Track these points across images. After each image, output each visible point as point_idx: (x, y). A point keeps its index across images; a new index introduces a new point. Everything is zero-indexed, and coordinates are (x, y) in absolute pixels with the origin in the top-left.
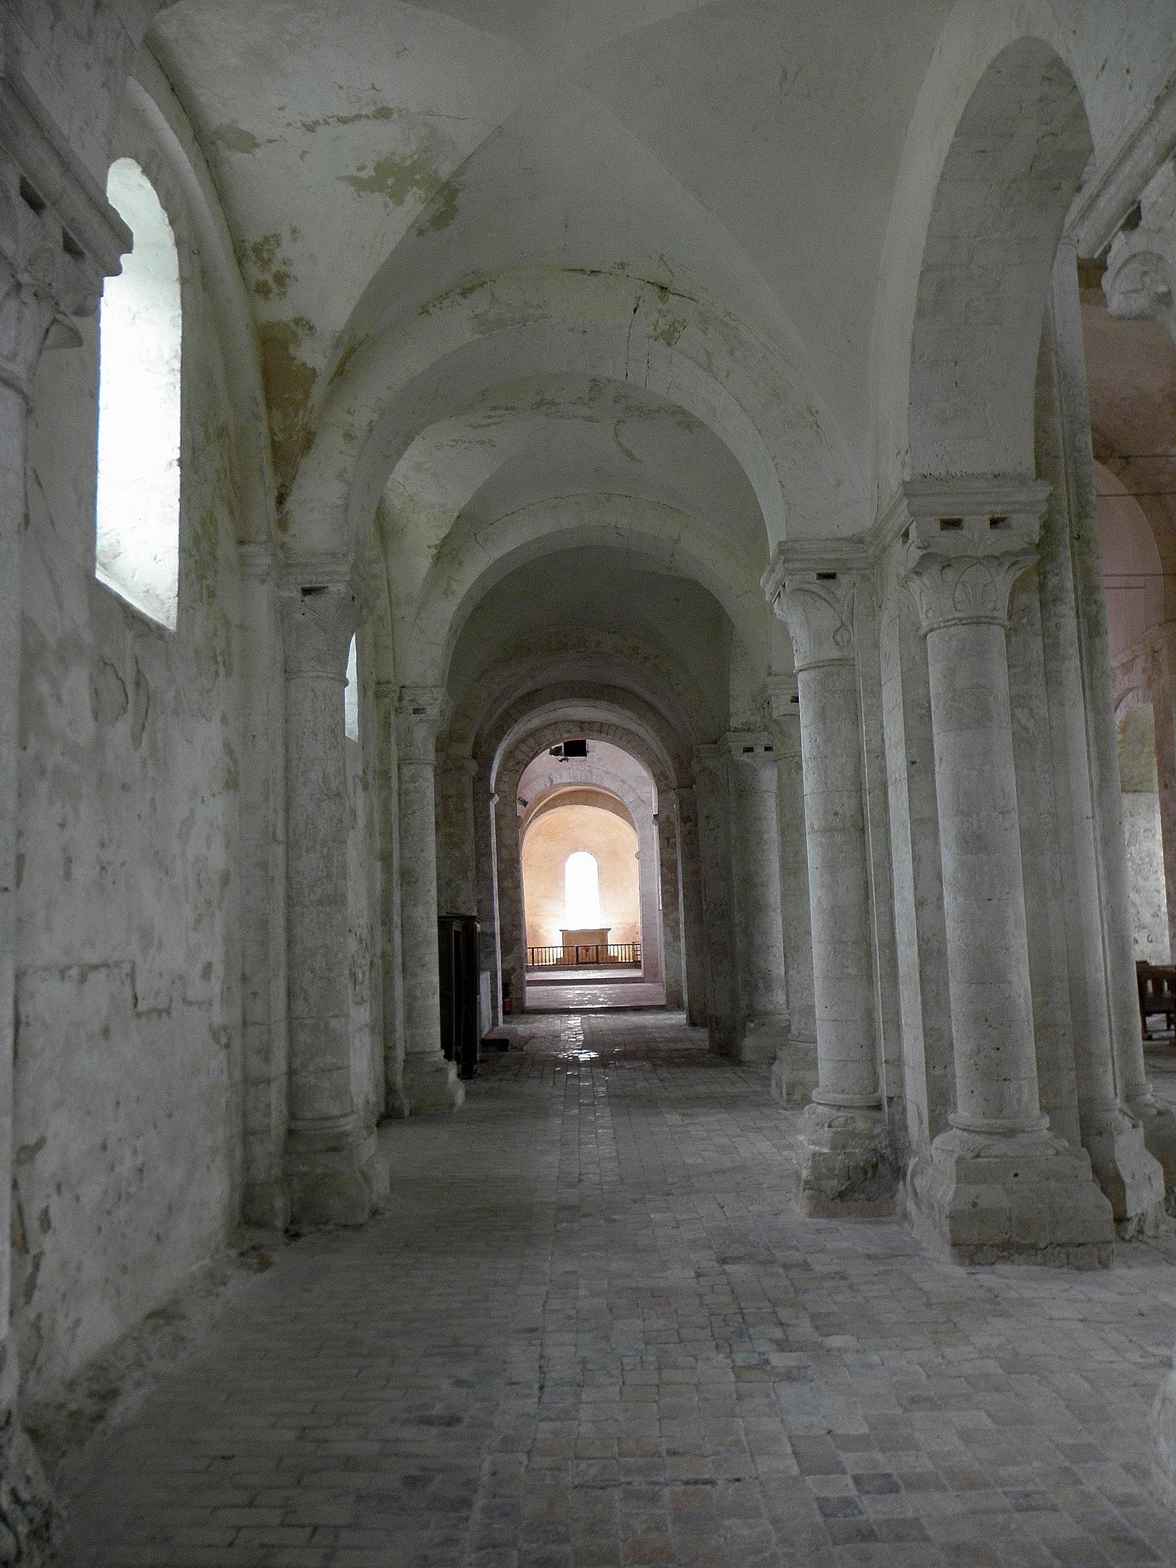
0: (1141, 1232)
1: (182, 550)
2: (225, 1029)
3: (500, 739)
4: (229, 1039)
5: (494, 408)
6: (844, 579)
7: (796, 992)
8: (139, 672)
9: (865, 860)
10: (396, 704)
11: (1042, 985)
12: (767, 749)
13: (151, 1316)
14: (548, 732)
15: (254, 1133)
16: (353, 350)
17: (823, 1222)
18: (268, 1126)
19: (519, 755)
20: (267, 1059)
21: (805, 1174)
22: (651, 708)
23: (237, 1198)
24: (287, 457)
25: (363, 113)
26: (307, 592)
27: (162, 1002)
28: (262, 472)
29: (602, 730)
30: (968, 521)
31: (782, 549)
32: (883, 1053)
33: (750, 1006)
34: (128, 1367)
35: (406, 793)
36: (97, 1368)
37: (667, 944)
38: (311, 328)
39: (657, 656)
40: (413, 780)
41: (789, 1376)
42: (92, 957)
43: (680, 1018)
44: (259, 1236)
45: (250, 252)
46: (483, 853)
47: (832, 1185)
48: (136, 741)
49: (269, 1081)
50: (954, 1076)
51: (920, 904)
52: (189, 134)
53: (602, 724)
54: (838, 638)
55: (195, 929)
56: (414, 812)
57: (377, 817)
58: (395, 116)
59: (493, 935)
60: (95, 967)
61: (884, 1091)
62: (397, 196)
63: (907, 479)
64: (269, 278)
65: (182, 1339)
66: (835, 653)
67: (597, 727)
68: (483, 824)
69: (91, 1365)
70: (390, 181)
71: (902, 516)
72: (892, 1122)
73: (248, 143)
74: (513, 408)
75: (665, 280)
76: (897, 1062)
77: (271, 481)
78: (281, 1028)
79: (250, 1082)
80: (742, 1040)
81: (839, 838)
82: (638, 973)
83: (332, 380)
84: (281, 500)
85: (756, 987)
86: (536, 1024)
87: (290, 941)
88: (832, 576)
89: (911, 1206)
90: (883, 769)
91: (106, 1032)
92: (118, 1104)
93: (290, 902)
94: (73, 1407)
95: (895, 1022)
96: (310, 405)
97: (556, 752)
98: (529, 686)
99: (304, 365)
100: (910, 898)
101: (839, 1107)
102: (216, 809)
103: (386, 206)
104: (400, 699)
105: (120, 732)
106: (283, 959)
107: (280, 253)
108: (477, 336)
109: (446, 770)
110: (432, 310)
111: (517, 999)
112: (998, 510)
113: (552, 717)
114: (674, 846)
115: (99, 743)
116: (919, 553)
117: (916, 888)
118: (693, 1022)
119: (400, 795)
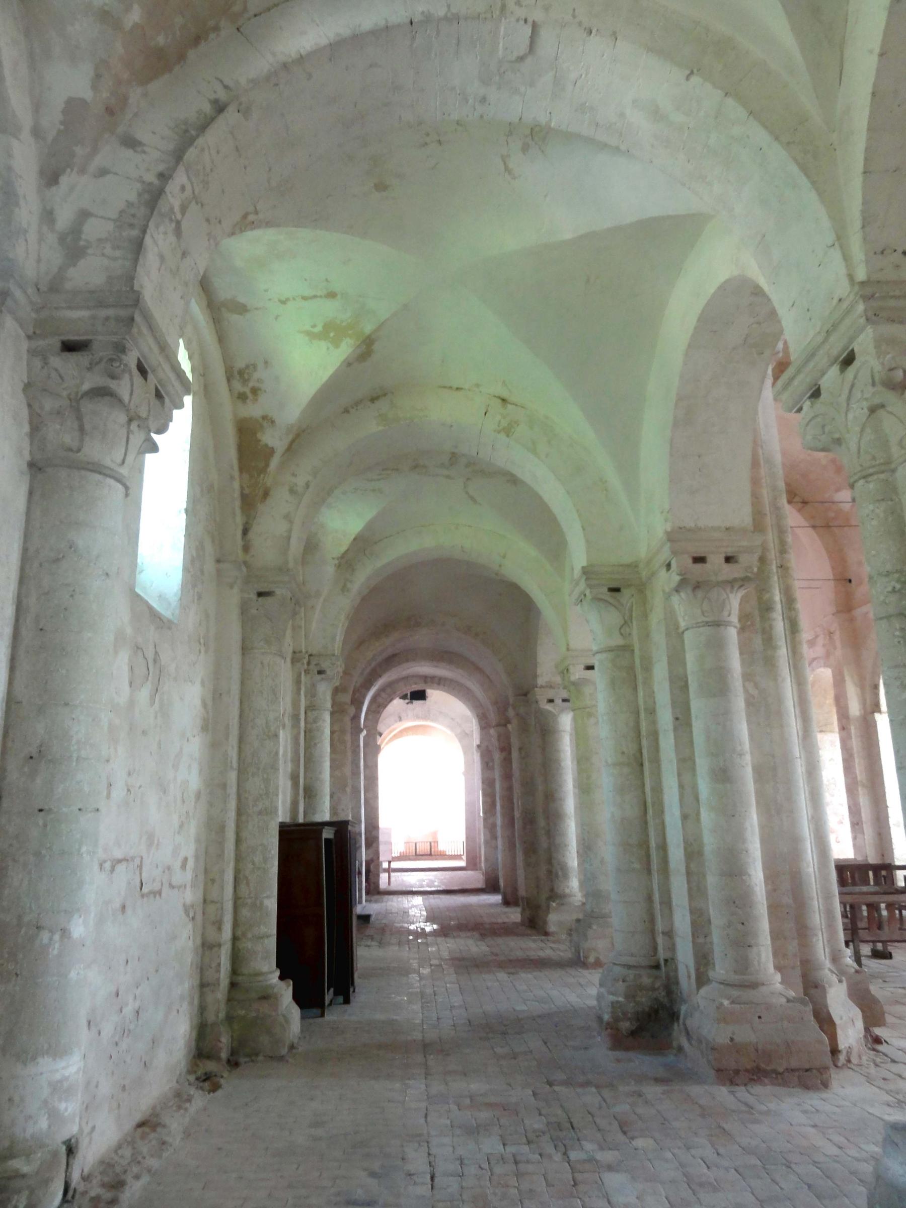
0: (849, 1061)
1: (186, 569)
2: (192, 906)
3: (368, 689)
4: (195, 913)
5: (383, 470)
6: (626, 593)
8: (156, 652)
9: (643, 785)
10: (306, 666)
11: (771, 877)
12: (564, 700)
13: (141, 1125)
15: (208, 985)
16: (298, 436)
17: (619, 1054)
18: (218, 979)
19: (380, 700)
20: (220, 929)
21: (606, 1017)
23: (194, 1035)
24: (251, 502)
25: (318, 294)
26: (260, 594)
27: (156, 886)
28: (234, 514)
30: (711, 558)
31: (587, 572)
32: (660, 926)
33: (552, 890)
34: (129, 1164)
36: (106, 1164)
37: (486, 842)
38: (273, 422)
40: (315, 721)
41: (610, 1168)
42: (118, 854)
43: (497, 898)
44: (211, 1066)
45: (236, 373)
46: (356, 773)
47: (625, 1026)
48: (152, 702)
49: (220, 946)
50: (712, 943)
51: (685, 817)
52: (205, 303)
54: (622, 631)
55: (179, 833)
56: (315, 744)
58: (339, 297)
60: (119, 861)
61: (662, 955)
62: (336, 343)
63: (669, 530)
64: (247, 390)
65: (164, 1143)
66: (620, 641)
69: (102, 1162)
70: (332, 335)
71: (665, 554)
72: (668, 977)
73: (242, 309)
74: (397, 470)
75: (505, 394)
76: (669, 934)
77: (239, 520)
78: (229, 906)
79: (207, 946)
80: (547, 916)
81: (626, 770)
82: (462, 863)
83: (283, 455)
84: (245, 532)
85: (557, 876)
86: (390, 903)
87: (238, 841)
88: (616, 590)
89: (684, 1042)
90: (654, 722)
91: (123, 907)
92: (127, 962)
93: (239, 813)
94: (93, 1194)
95: (667, 902)
96: (268, 470)
97: (404, 697)
98: (390, 652)
99: (266, 445)
100: (677, 812)
101: (629, 967)
102: (194, 747)
103: (328, 349)
104: (309, 663)
105: (144, 694)
106: (232, 855)
107: (256, 375)
108: (380, 428)
109: (337, 711)
110: (351, 410)
112: (730, 551)
113: (405, 673)
115: (131, 704)
116: (678, 578)
117: (681, 807)
118: (506, 903)
119: (305, 732)
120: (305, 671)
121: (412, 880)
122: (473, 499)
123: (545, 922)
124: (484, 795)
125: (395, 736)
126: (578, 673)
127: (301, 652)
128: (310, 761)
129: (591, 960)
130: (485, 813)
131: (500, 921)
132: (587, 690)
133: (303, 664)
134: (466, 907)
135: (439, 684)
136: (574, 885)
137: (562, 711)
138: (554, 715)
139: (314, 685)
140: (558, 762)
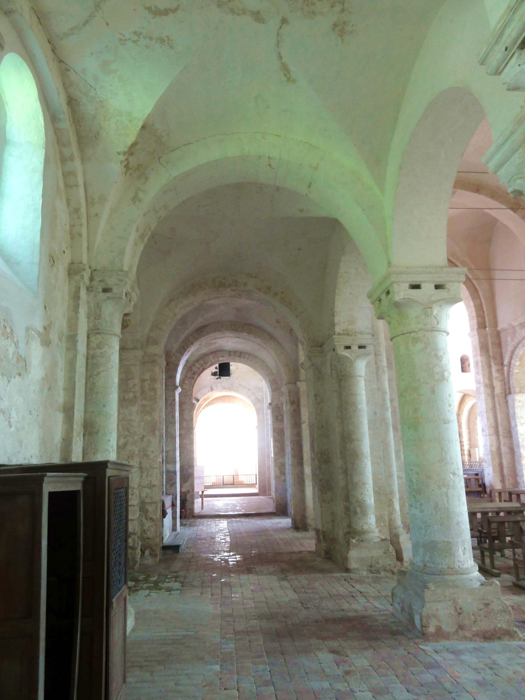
3: (182, 354)
7: (420, 528)
10: (88, 283)
12: (360, 347)
14: (211, 357)
19: (194, 369)
22: (272, 337)
29: (240, 355)
33: (349, 526)
35: (93, 357)
37: (277, 478)
39: (283, 293)
40: (99, 346)
43: (286, 522)
46: (170, 422)
53: (241, 353)
56: (99, 373)
57: (61, 375)
59: (175, 473)
67: (238, 354)
68: (171, 404)
82: (255, 490)
85: (355, 513)
86: (200, 527)
97: (214, 374)
98: (200, 321)
104: (91, 279)
111: (190, 509)
113: (213, 347)
114: (282, 420)
120: (88, 289)
121: (220, 505)
122: (285, 69)
123: (346, 559)
124: (275, 441)
125: (208, 403)
126: (402, 292)
127: (81, 263)
128: (91, 392)
129: (432, 629)
130: (275, 454)
131: (296, 549)
132: (413, 313)
133: (82, 277)
134: (263, 531)
135: (240, 357)
136: (371, 522)
137: (358, 357)
138: (352, 361)
139: (98, 306)
140: (354, 404)
